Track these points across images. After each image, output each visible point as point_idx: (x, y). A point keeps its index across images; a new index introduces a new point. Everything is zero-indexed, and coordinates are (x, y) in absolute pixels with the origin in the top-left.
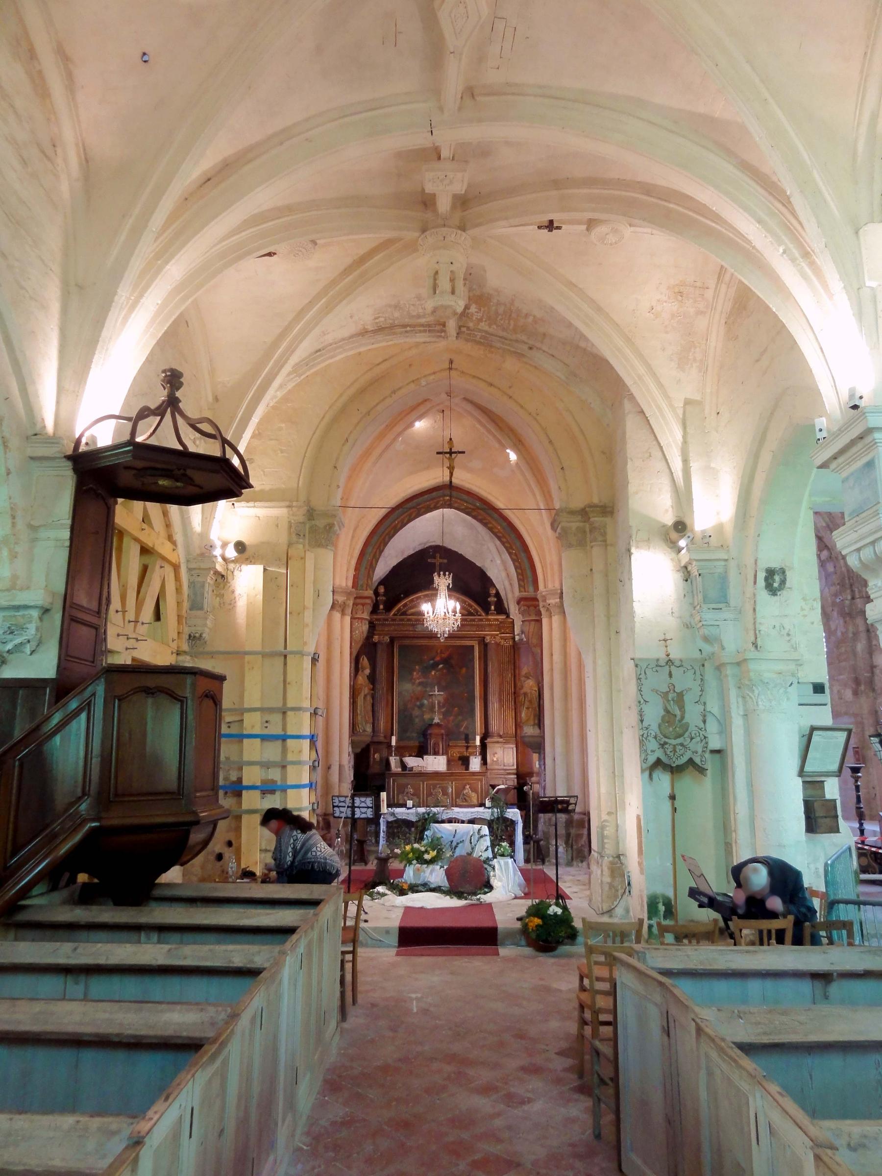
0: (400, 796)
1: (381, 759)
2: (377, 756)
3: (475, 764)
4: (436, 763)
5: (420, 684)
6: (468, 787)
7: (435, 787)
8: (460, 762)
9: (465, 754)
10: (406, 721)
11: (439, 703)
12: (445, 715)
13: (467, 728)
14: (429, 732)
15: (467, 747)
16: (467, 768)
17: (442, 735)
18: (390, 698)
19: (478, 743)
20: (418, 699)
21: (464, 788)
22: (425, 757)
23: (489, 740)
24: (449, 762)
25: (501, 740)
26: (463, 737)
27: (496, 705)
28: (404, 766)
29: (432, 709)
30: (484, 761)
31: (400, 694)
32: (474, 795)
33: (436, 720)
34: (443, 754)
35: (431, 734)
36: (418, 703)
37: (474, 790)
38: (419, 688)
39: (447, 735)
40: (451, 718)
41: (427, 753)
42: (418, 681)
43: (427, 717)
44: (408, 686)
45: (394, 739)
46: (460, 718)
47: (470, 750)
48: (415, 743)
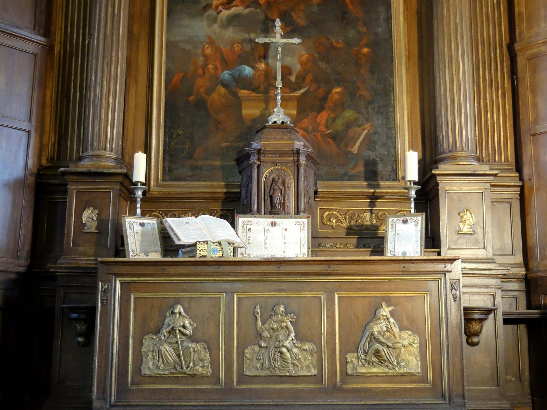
0: (148, 343)
1: (102, 223)
2: (89, 216)
3: (404, 237)
4: (279, 237)
5: (233, 20)
6: (385, 311)
7: (270, 313)
8: (353, 240)
9: (367, 219)
10: (187, 113)
11: (286, 71)
12: (306, 107)
13: (370, 143)
14: (256, 145)
15: (373, 199)
16: (379, 249)
17: (298, 152)
18: (143, 57)
19: (412, 171)
20: (226, 64)
21: (374, 316)
22: (241, 220)
23: (442, 169)
24: (316, 239)
25: (484, 169)
26: (361, 168)
27: (465, 69)
28: (166, 240)
29: (263, 88)
30: (432, 239)
31: (171, 46)
32: (407, 338)
33: (278, 115)
34: (297, 212)
35: (259, 151)
36: (226, 75)
37: (408, 324)
38: (230, 33)
39: (309, 157)
40: (324, 117)
41: (247, 210)
42: (225, 13)
43: (250, 111)
44: (199, 29)
45: (140, 159)
46: (349, 114)
47: (380, 206)
48: (218, 187)
